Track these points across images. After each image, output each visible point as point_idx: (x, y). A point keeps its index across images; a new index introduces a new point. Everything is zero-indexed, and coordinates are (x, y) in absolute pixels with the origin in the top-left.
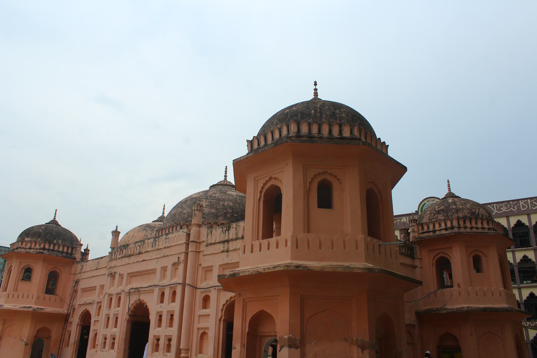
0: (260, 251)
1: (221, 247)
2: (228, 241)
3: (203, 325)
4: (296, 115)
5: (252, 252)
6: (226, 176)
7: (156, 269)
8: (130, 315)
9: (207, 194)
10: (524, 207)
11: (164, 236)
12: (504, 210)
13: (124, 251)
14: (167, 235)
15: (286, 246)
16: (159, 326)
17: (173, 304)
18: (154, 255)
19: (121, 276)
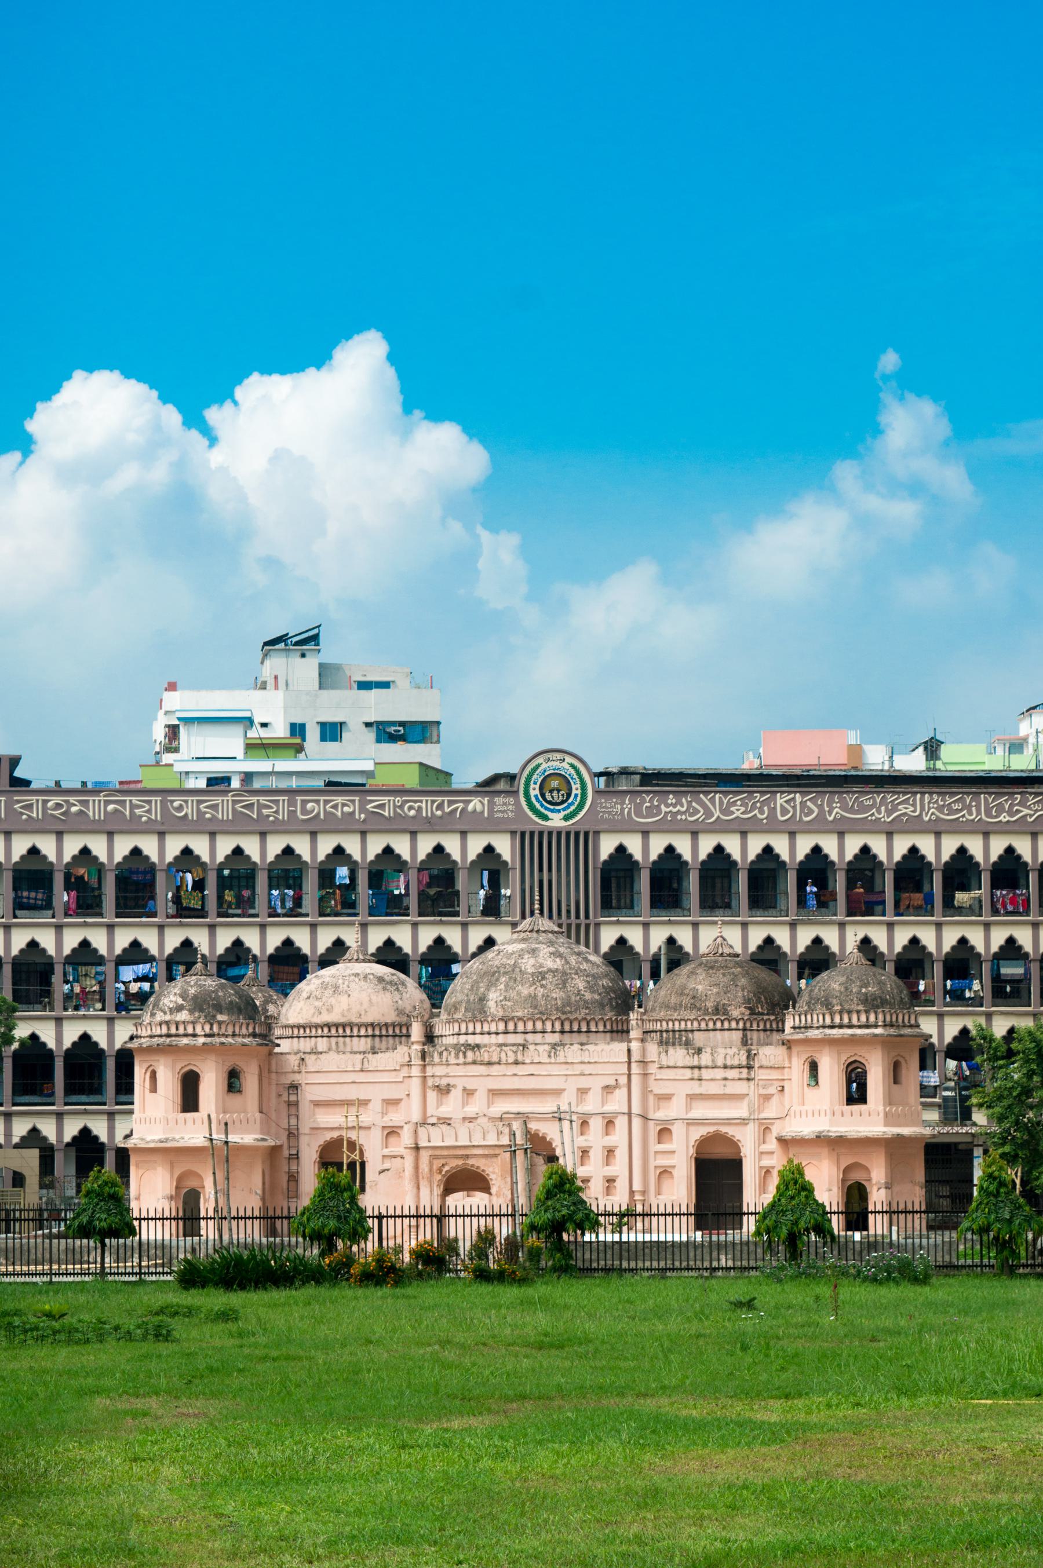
1: (688, 1073)
2: (700, 1068)
3: (663, 1161)
4: (875, 999)
7: (564, 1090)
9: (567, 962)
10: (784, 812)
11: (576, 1047)
12: (737, 814)
13: (470, 1054)
18: (556, 1070)
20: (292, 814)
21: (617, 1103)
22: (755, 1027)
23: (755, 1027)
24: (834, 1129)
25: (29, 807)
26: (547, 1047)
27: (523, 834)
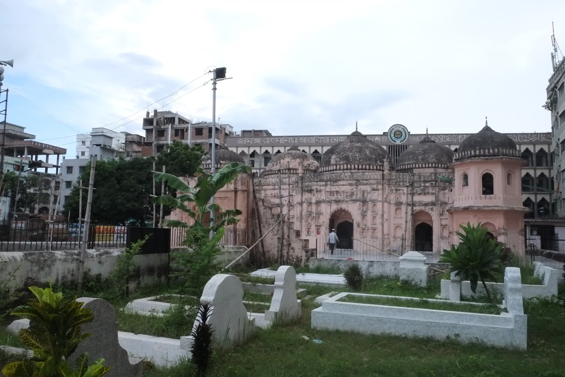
6: (357, 128)
8: (331, 216)
10: (461, 140)
20: (330, 141)
21: (377, 196)
22: (440, 166)
23: (440, 166)
24: (476, 205)
25: (266, 140)
26: (349, 174)
27: (389, 146)
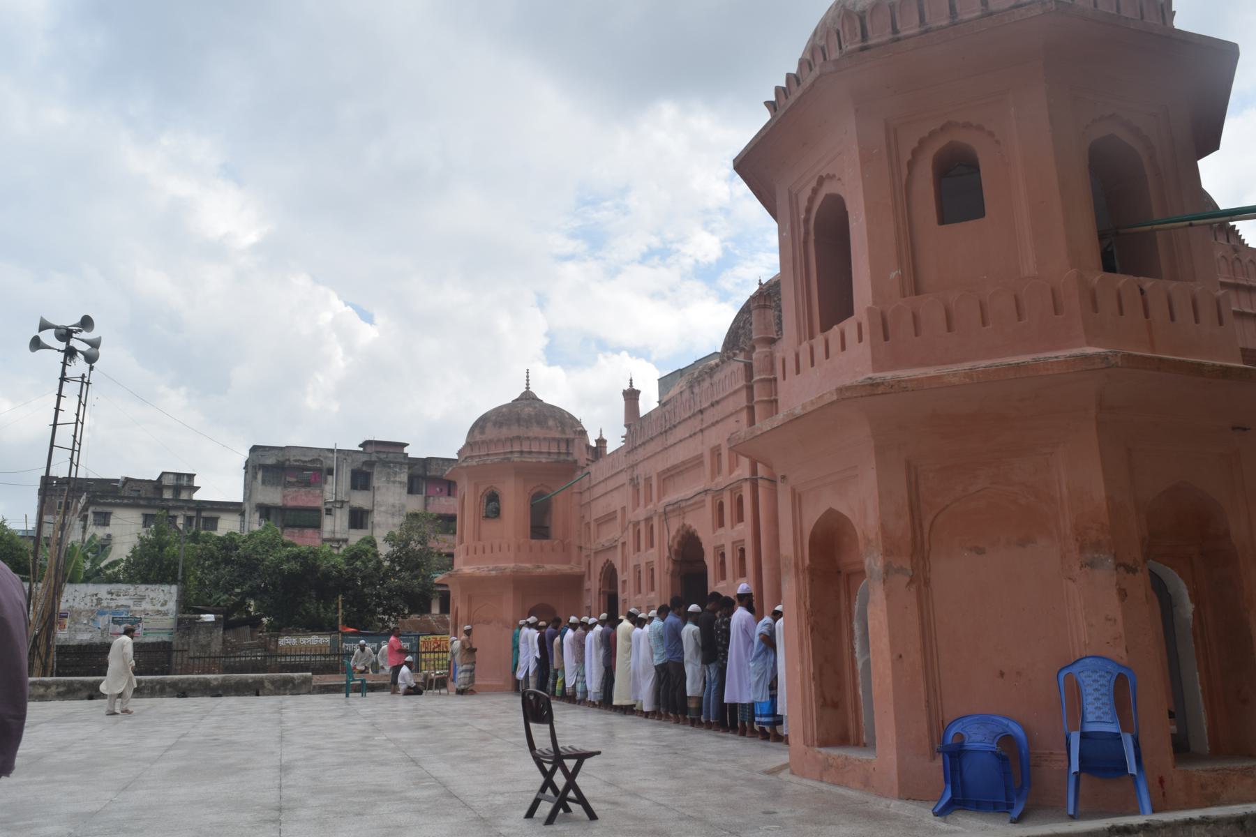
0: (812, 365)
5: (798, 372)
7: (702, 455)
8: (675, 562)
14: (711, 377)
15: (860, 340)
16: (723, 577)
17: (740, 526)
19: (648, 480)
